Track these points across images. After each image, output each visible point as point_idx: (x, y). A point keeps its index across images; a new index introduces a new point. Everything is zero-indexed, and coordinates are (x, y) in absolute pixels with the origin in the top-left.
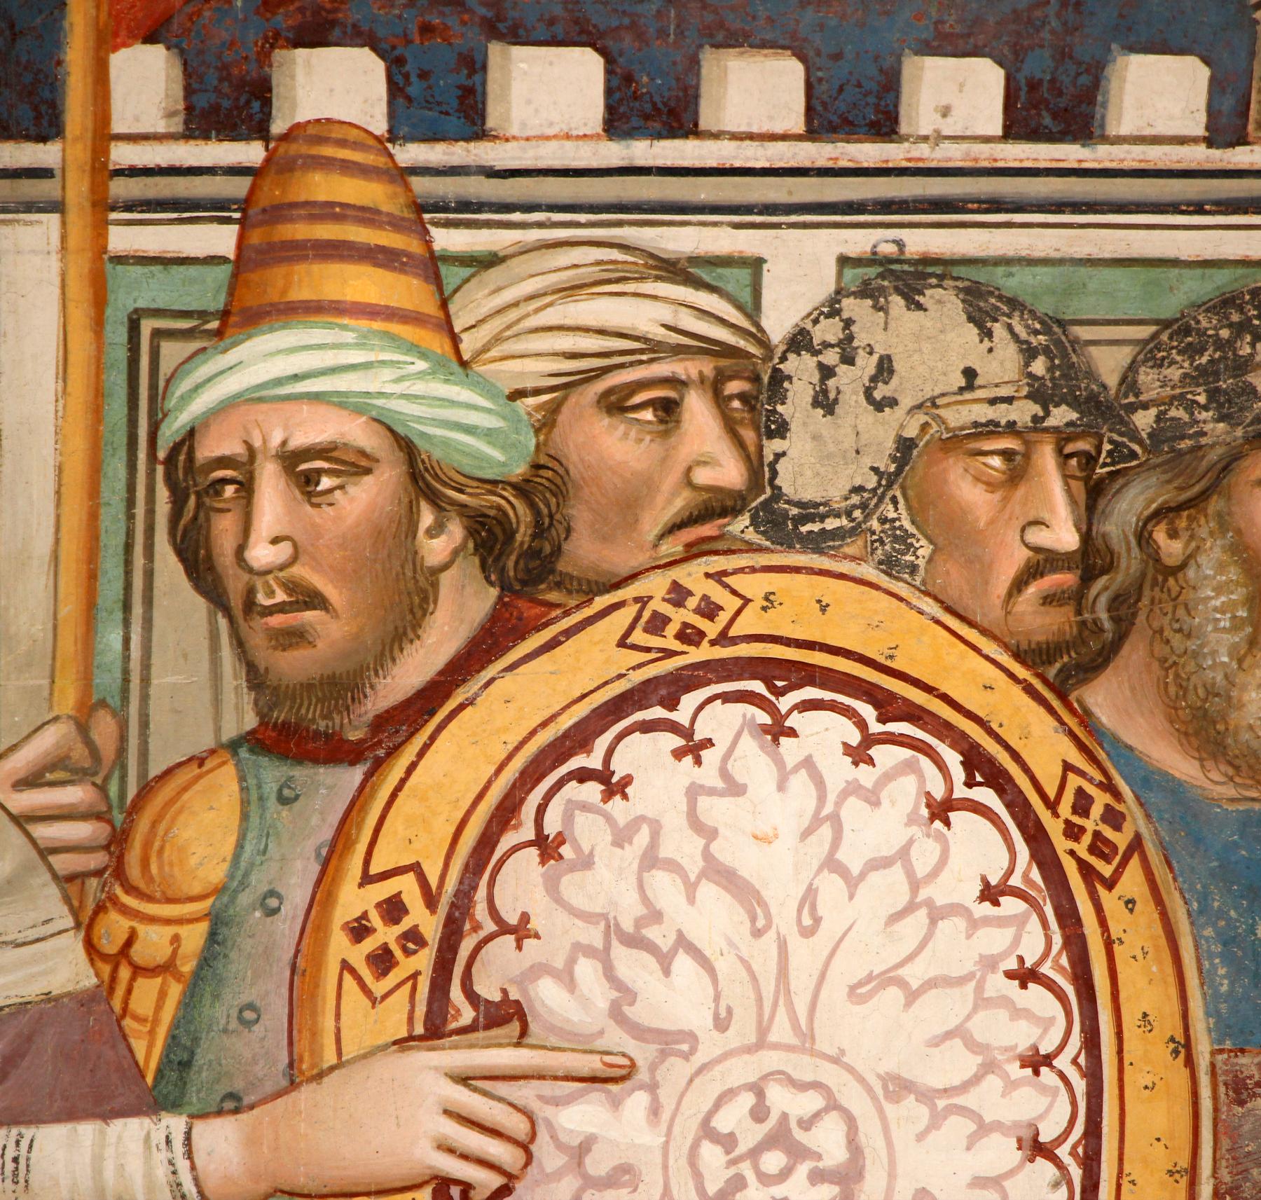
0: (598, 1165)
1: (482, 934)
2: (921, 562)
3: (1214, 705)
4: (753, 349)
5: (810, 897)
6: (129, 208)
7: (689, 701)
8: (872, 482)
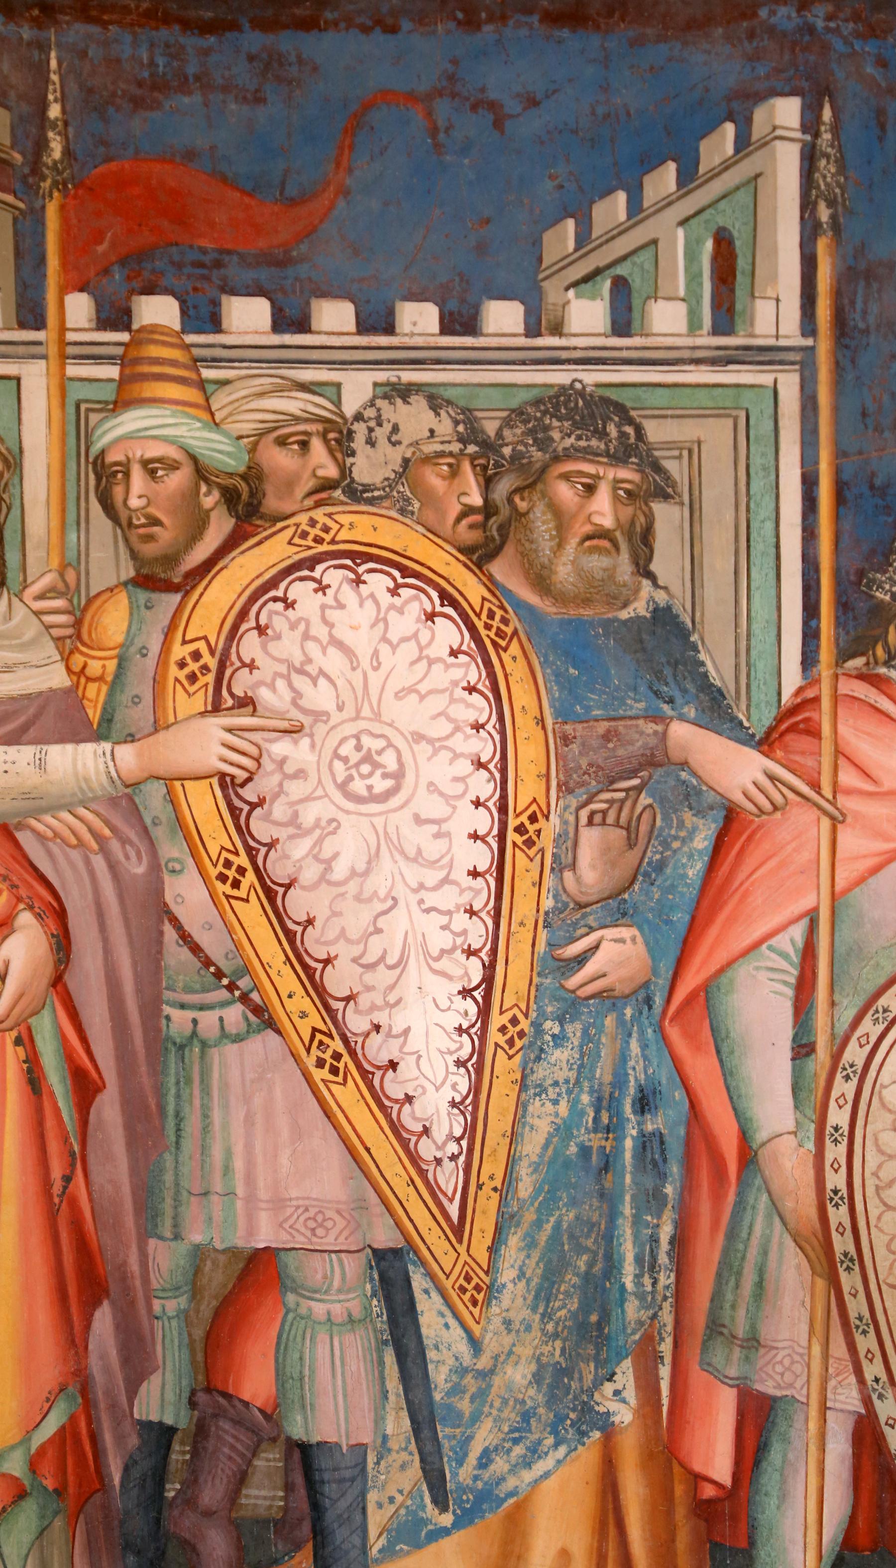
0: (289, 768)
1: (235, 667)
2: (416, 510)
3: (545, 573)
4: (339, 420)
5: (376, 653)
6: (74, 358)
7: (320, 568)
8: (393, 476)
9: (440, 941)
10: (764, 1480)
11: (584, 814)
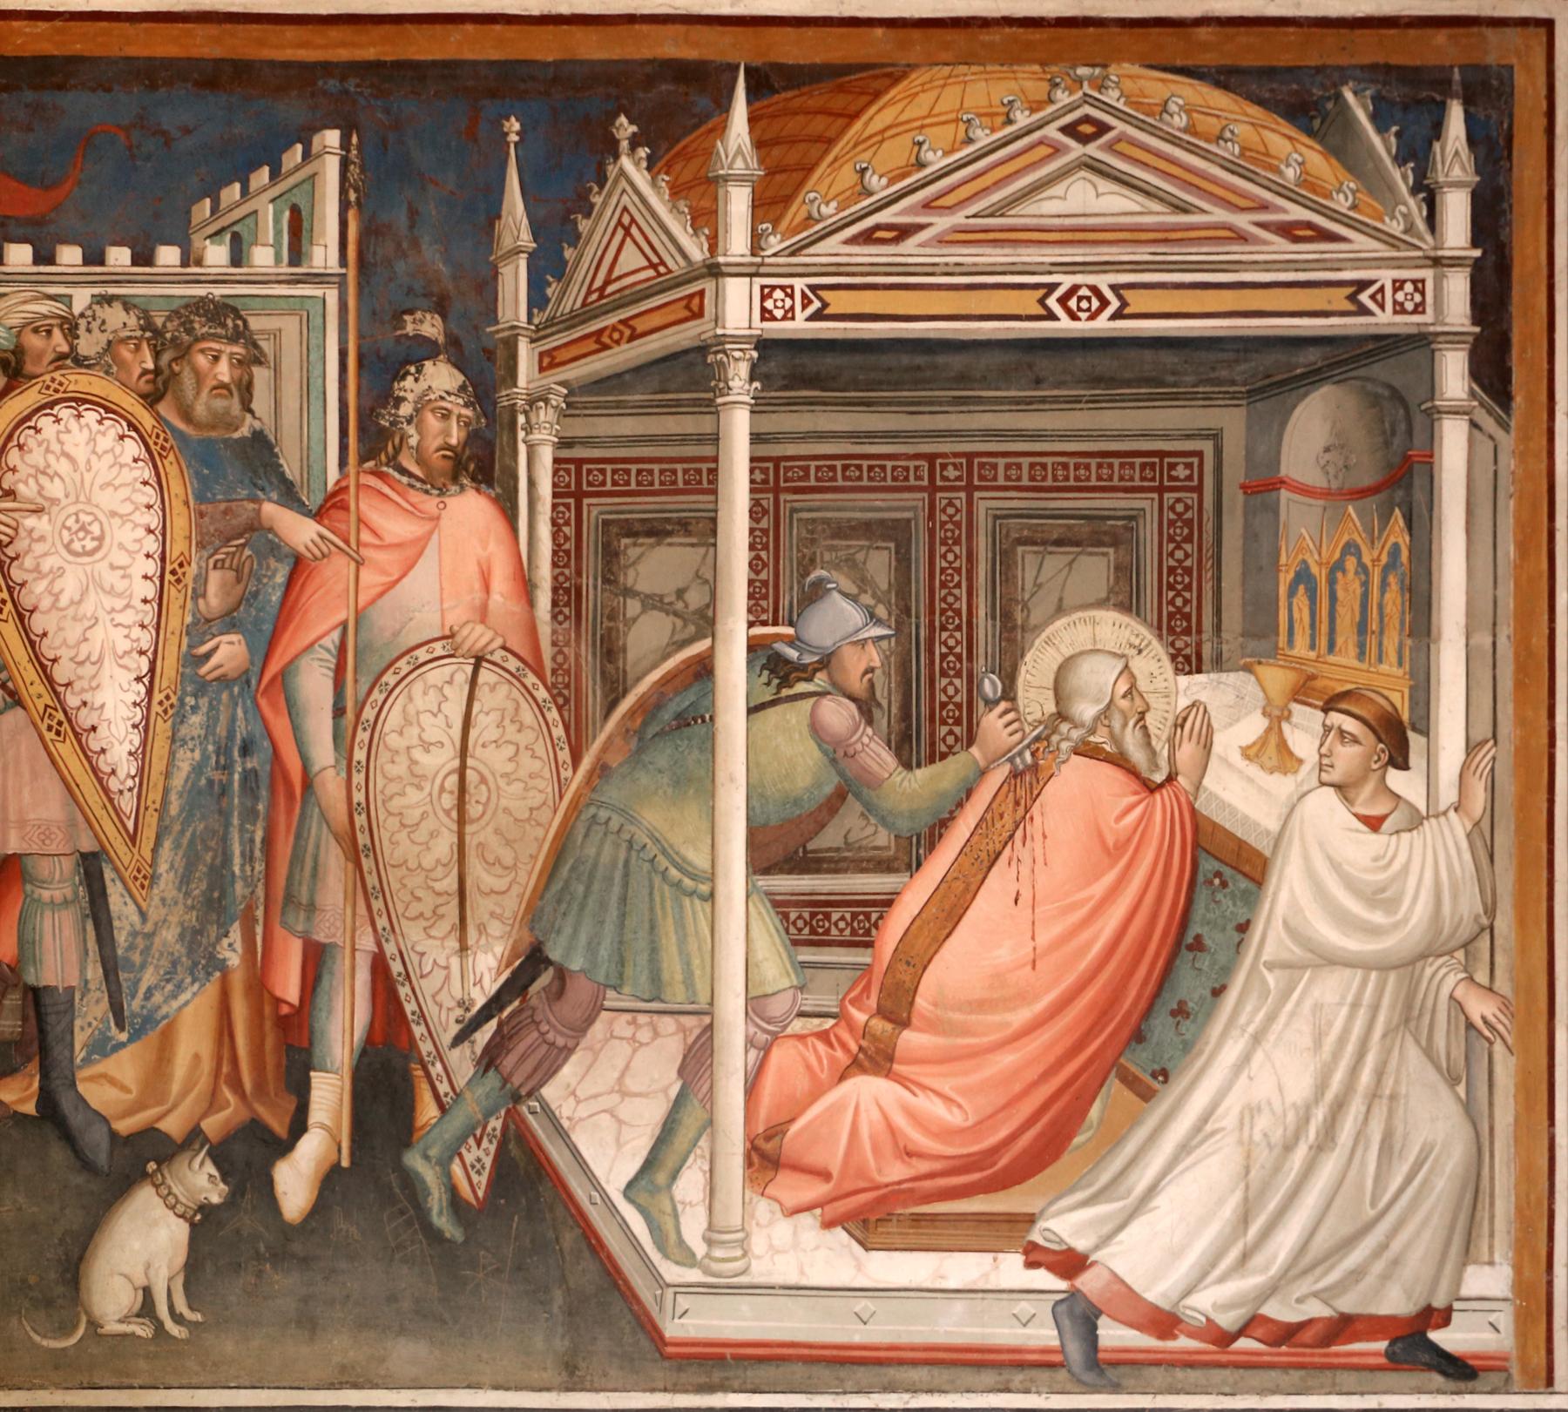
0: (35, 535)
5: (88, 461)
7: (57, 408)
9: (123, 645)
10: (318, 1000)
11: (211, 562)
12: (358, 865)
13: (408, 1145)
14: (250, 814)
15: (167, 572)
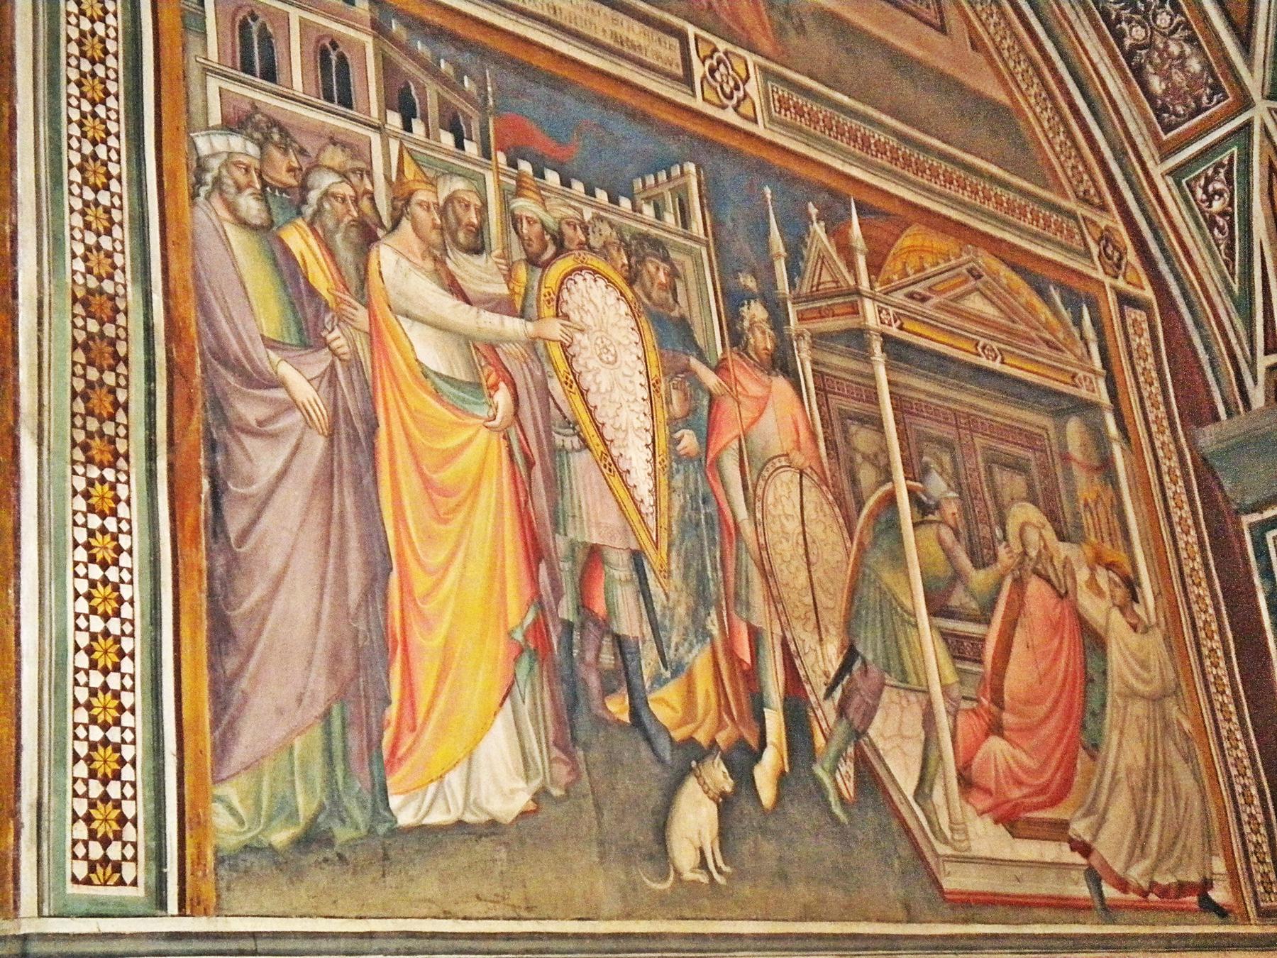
9: (637, 424)
12: (767, 580)
13: (815, 761)
14: (712, 541)
15: (652, 386)
